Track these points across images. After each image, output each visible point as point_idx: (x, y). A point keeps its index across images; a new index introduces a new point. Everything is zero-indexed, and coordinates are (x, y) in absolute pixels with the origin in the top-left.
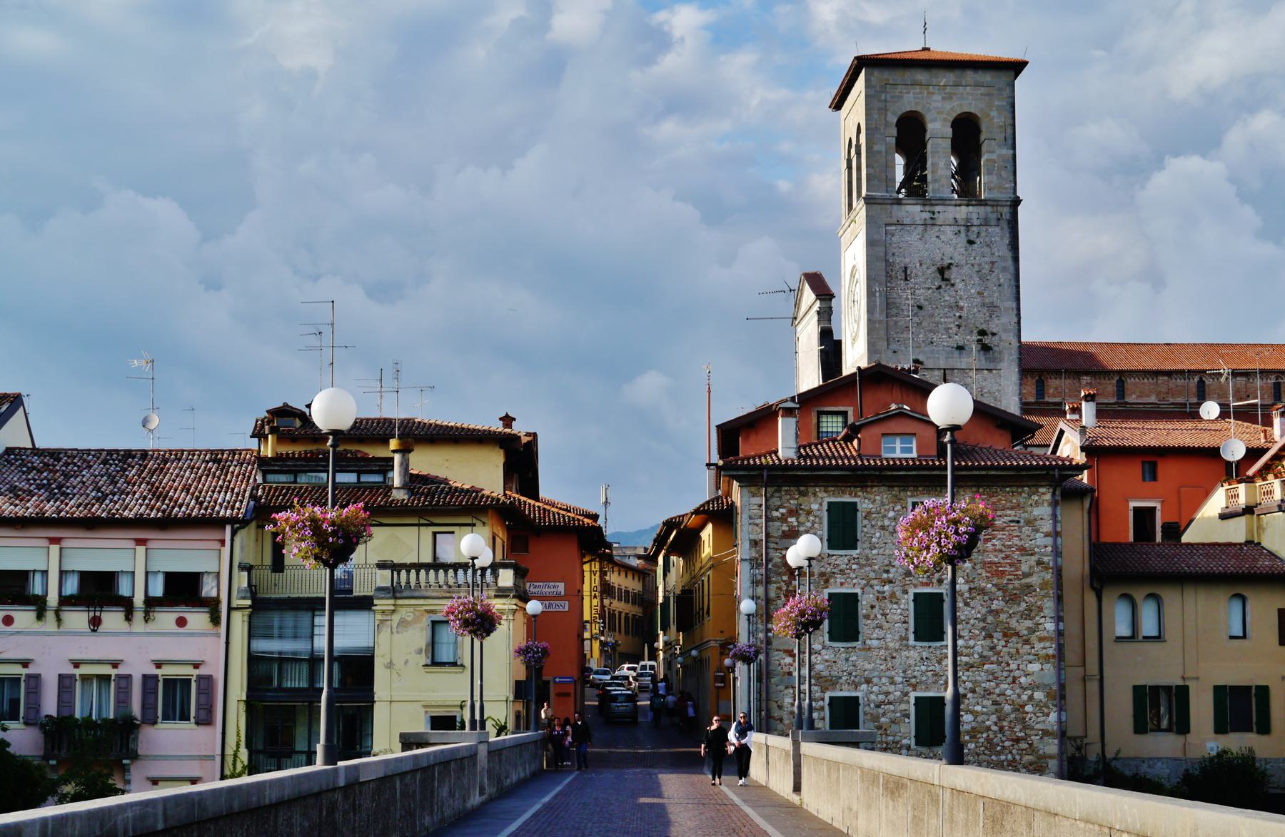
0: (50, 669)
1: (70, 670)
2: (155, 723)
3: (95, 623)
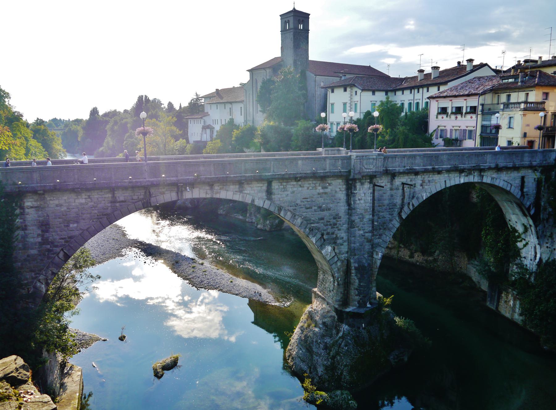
0: (448, 128)
1: (452, 128)
2: (466, 140)
3: (456, 118)
